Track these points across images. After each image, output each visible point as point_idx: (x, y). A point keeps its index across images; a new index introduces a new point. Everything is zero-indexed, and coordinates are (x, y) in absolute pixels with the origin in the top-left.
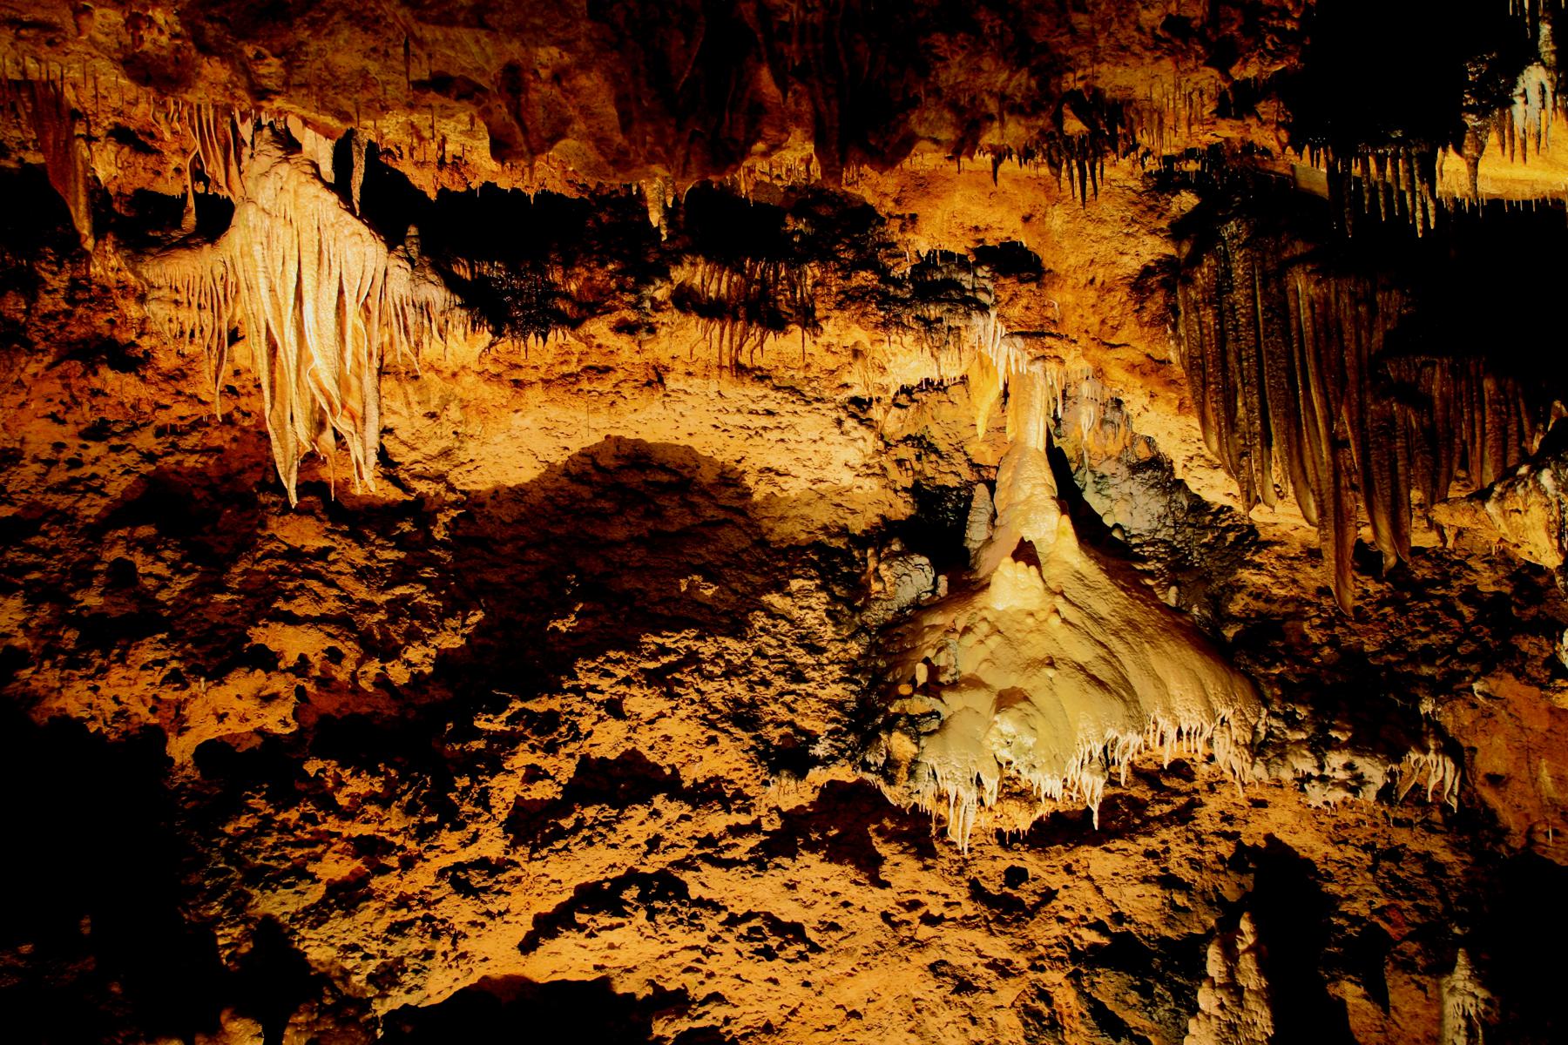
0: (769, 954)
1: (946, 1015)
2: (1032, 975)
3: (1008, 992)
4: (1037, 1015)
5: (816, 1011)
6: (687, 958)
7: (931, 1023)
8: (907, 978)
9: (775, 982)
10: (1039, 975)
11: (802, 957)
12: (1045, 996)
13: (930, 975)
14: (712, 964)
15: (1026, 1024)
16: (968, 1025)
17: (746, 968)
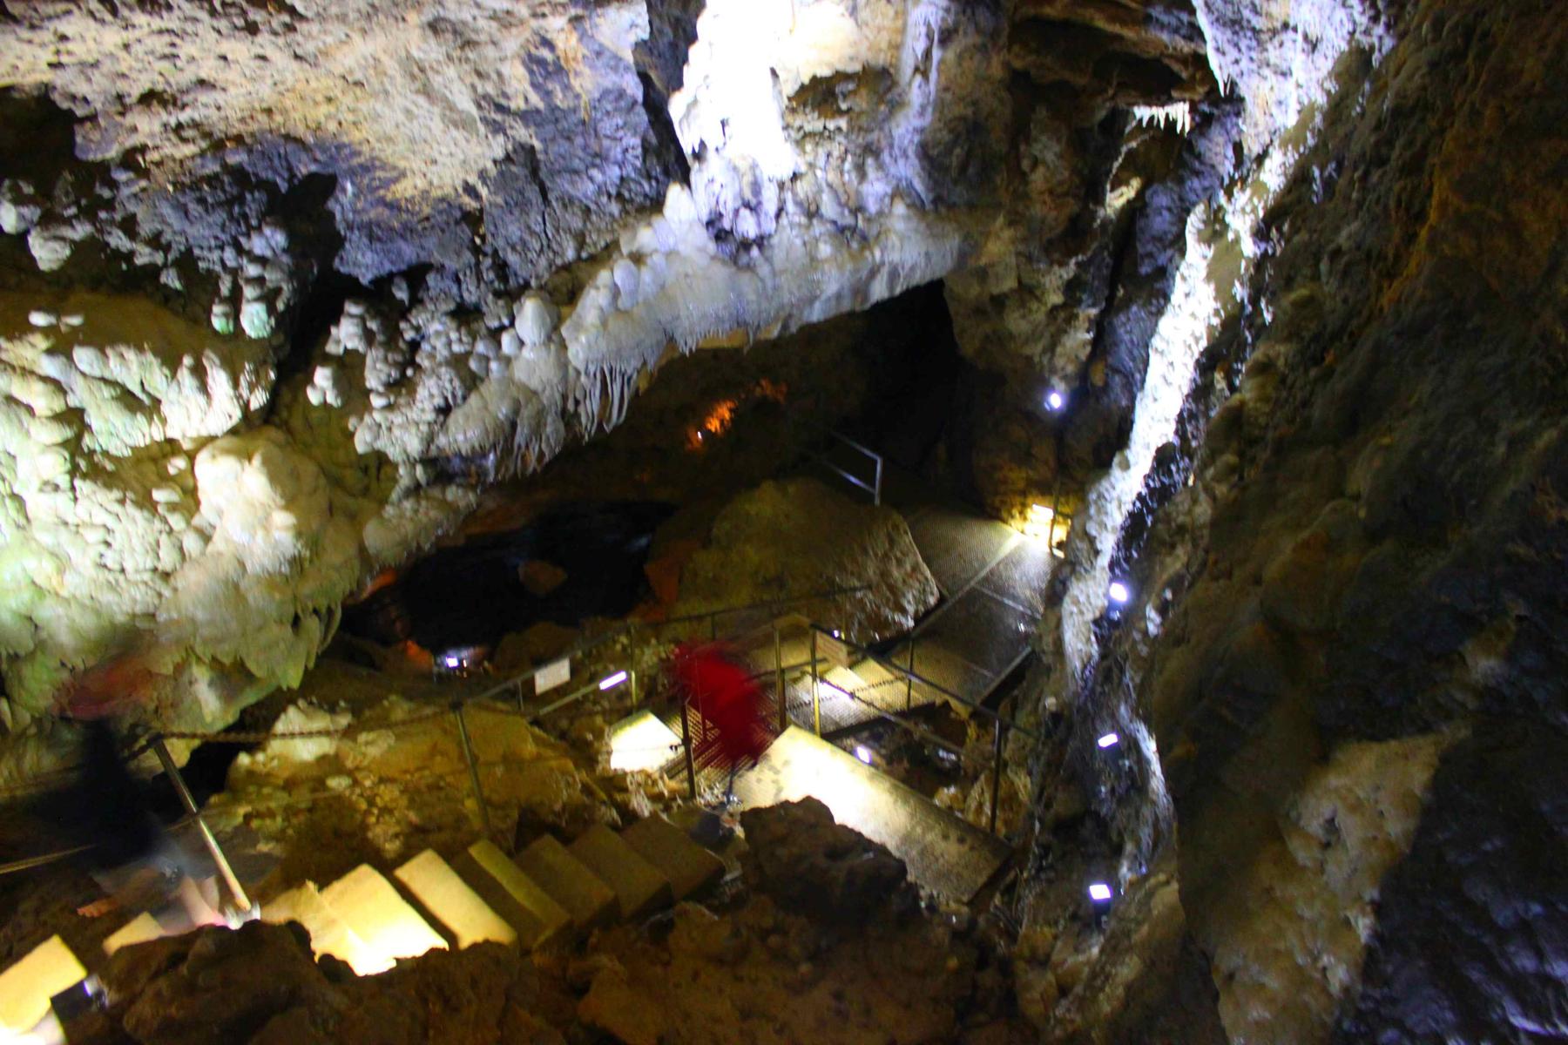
0: (252, 29)
1: (451, 71)
2: (534, 23)
3: (513, 43)
4: (541, 62)
5: (313, 84)
6: (160, 44)
7: (437, 81)
8: (413, 38)
9: (263, 58)
10: (542, 22)
11: (290, 28)
12: (548, 44)
13: (429, 33)
14: (186, 49)
15: (531, 72)
16: (476, 81)
17: (227, 47)
